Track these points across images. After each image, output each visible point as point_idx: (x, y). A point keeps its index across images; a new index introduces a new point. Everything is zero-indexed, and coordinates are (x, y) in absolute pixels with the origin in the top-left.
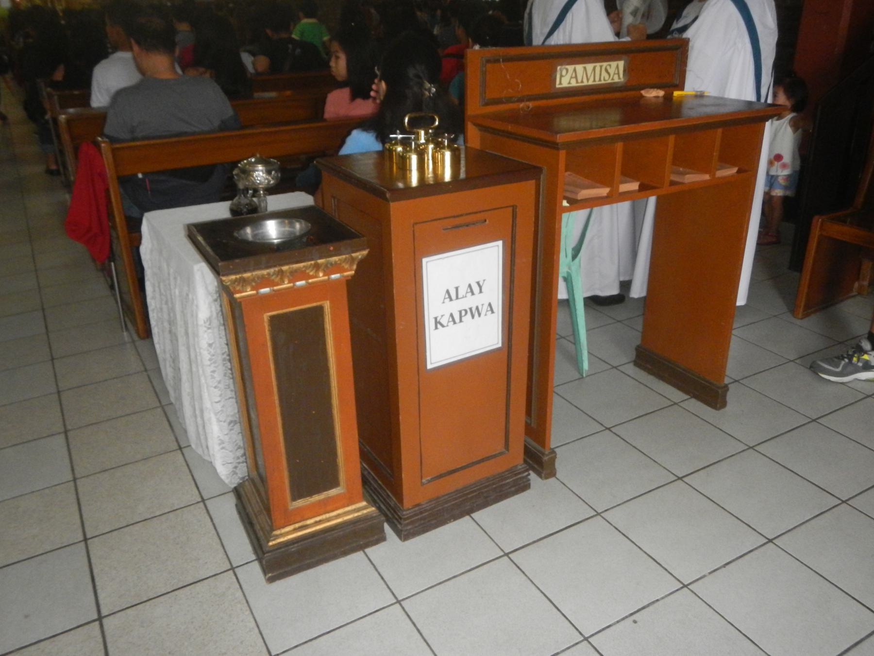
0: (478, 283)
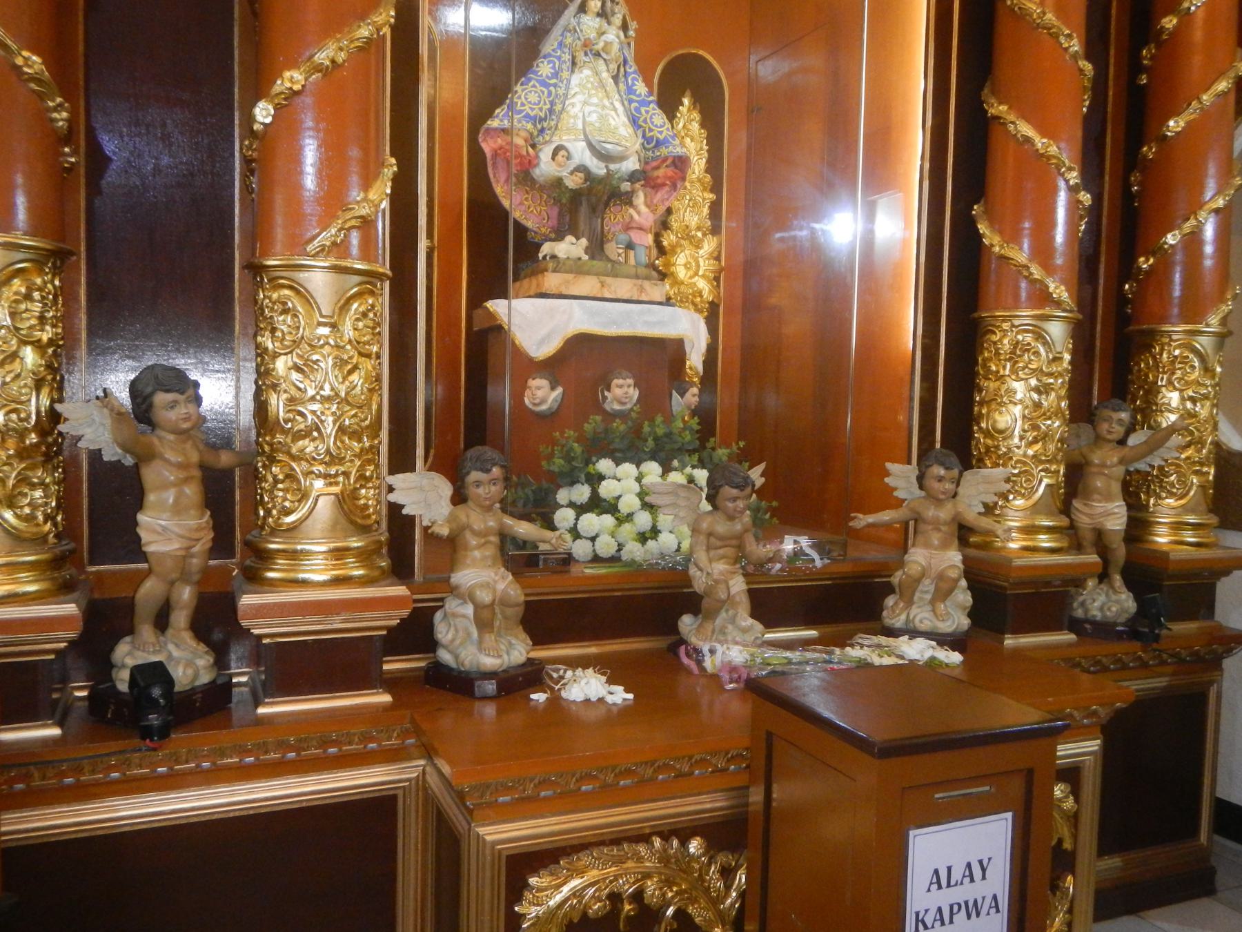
0: (981, 862)
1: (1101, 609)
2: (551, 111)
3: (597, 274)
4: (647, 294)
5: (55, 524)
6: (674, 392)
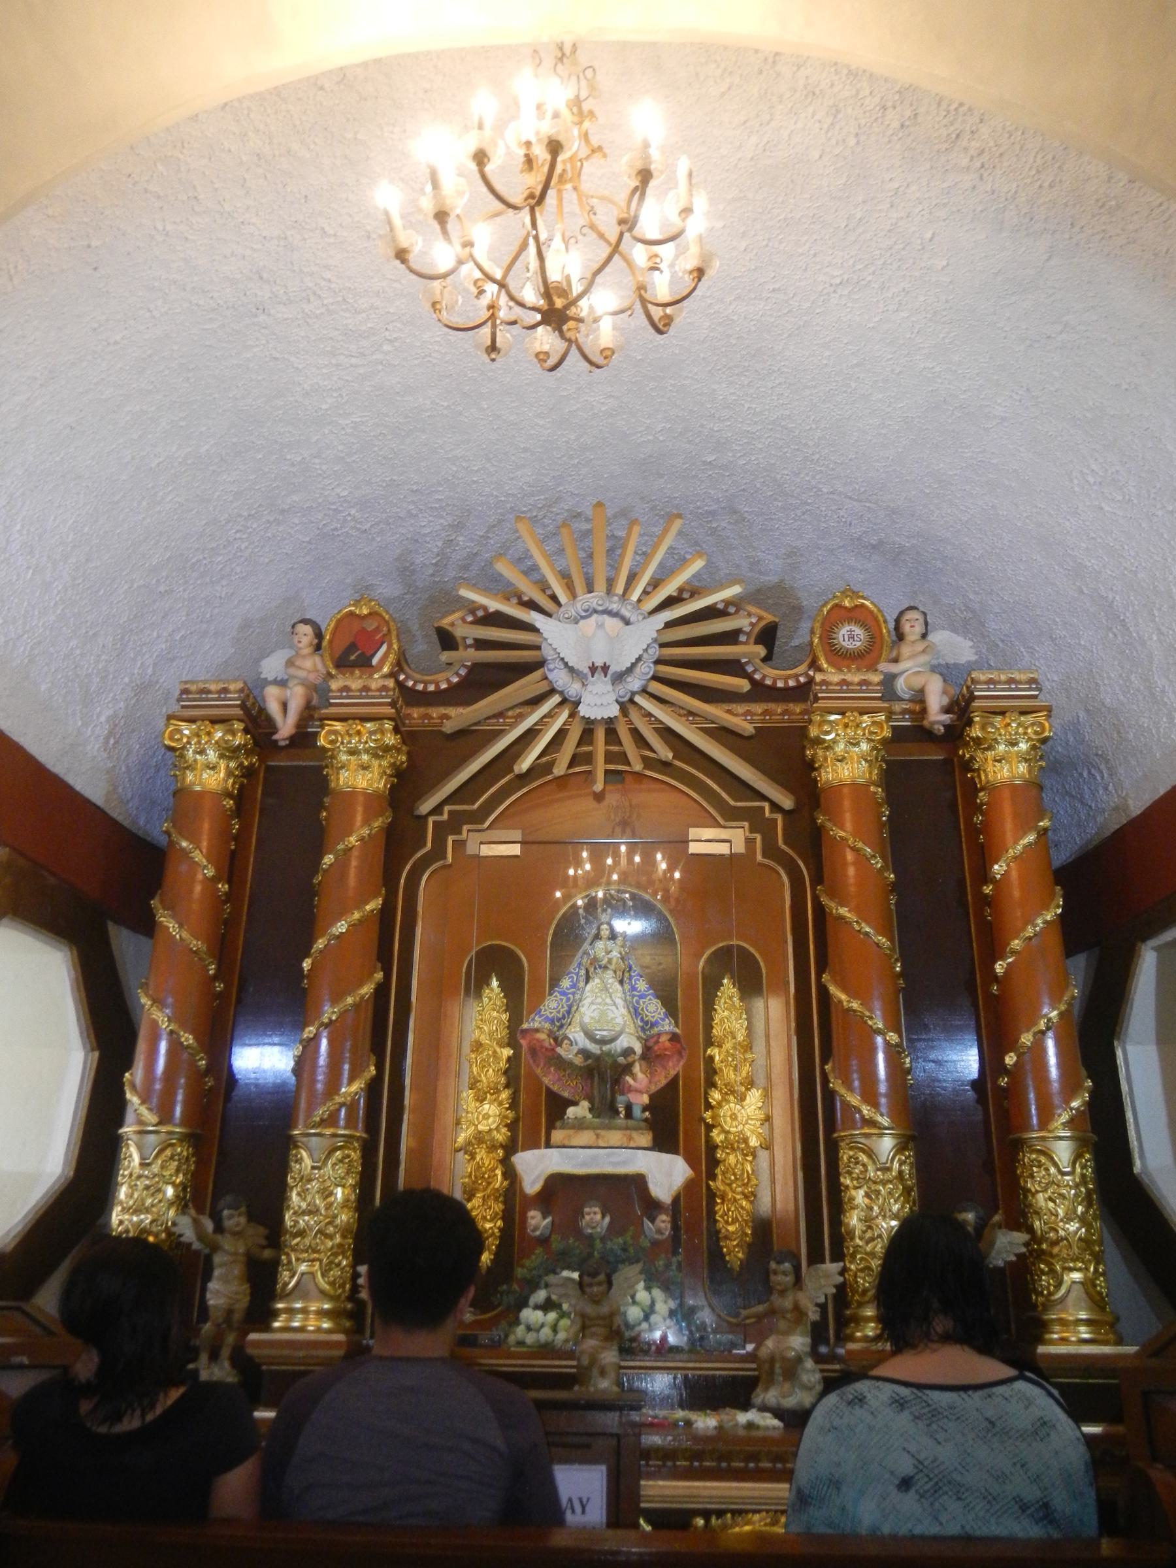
0: (581, 1500)
2: (569, 1012)
3: (594, 1128)
4: (635, 1142)
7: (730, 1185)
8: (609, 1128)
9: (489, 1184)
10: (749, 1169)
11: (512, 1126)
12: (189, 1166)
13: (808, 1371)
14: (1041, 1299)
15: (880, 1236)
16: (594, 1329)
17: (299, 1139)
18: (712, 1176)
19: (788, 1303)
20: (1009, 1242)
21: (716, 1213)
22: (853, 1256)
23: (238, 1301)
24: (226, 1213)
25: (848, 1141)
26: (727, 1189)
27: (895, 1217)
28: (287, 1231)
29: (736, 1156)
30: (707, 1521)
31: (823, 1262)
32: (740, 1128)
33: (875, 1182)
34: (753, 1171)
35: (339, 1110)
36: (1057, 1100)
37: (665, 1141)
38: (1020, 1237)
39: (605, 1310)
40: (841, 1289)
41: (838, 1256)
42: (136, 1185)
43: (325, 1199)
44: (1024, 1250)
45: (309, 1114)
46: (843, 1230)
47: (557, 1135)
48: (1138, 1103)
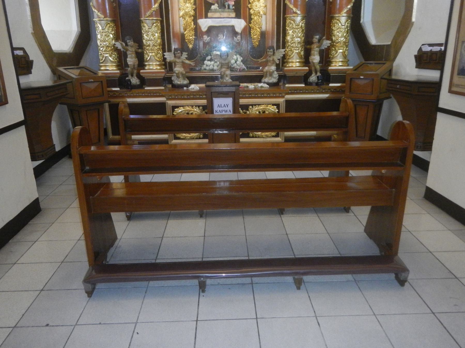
0: (227, 105)
1: (312, 80)
5: (117, 60)
6: (234, 37)
7: (255, 25)
8: (223, 12)
9: (190, 26)
10: (260, 20)
11: (195, 10)
12: (114, 28)
13: (275, 74)
14: (332, 56)
15: (295, 42)
16: (224, 66)
17: (144, 21)
18: (251, 23)
19: (271, 59)
20: (326, 43)
21: (251, 33)
22: (288, 47)
23: (135, 63)
24: (128, 41)
25: (289, 18)
26: (254, 26)
27: (299, 37)
28: (145, 45)
29: (257, 17)
30: (252, 107)
31: (280, 49)
32: (258, 9)
33: (295, 29)
34: (261, 21)
35: (153, 12)
36: (344, 6)
37: (238, 16)
38: (329, 42)
39: (227, 62)
40: (284, 55)
41: (284, 47)
42: (102, 35)
43: (153, 37)
44: (329, 45)
45: (145, 14)
46: (286, 40)
47: (210, 15)
48: (365, 4)
